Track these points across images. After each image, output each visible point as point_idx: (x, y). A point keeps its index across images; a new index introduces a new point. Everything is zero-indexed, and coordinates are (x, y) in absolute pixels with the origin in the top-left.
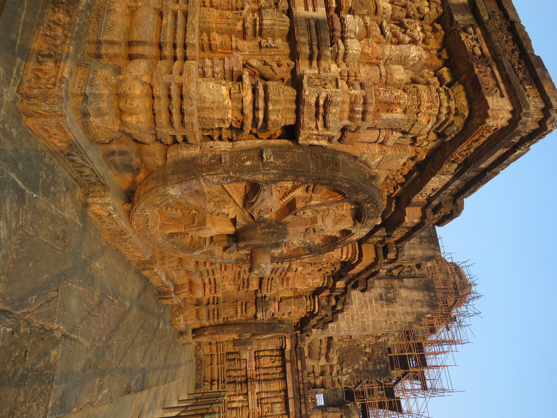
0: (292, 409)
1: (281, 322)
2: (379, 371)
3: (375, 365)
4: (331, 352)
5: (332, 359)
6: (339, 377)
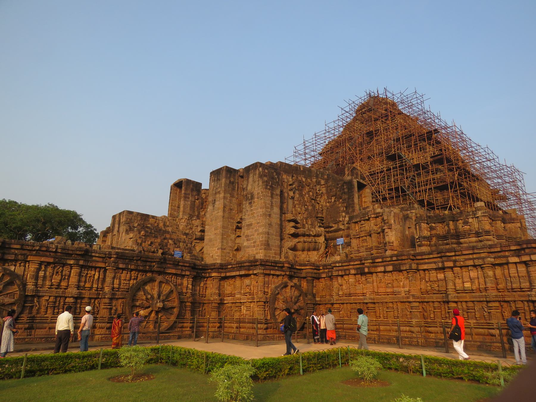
3: (345, 193)
4: (311, 233)
6: (345, 223)
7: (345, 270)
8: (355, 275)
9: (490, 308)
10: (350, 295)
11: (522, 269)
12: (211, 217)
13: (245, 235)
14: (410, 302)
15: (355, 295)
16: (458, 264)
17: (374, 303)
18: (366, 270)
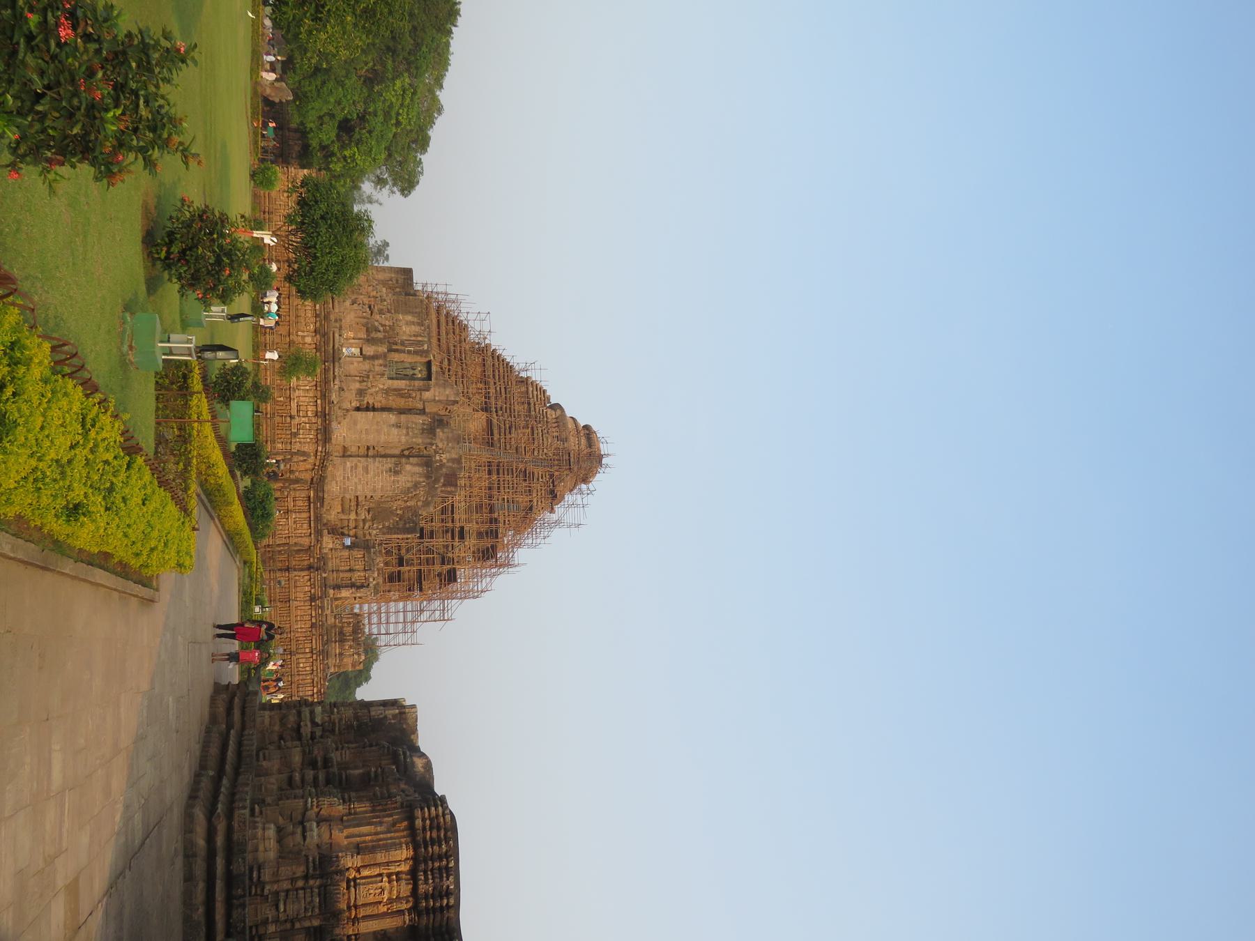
0: (312, 526)
1: (302, 480)
2: (408, 529)
5: (360, 514)
7: (314, 584)
8: (310, 591)
11: (310, 693)
12: (382, 422)
13: (359, 464)
14: (290, 632)
16: (314, 661)
17: (289, 607)
18: (313, 604)
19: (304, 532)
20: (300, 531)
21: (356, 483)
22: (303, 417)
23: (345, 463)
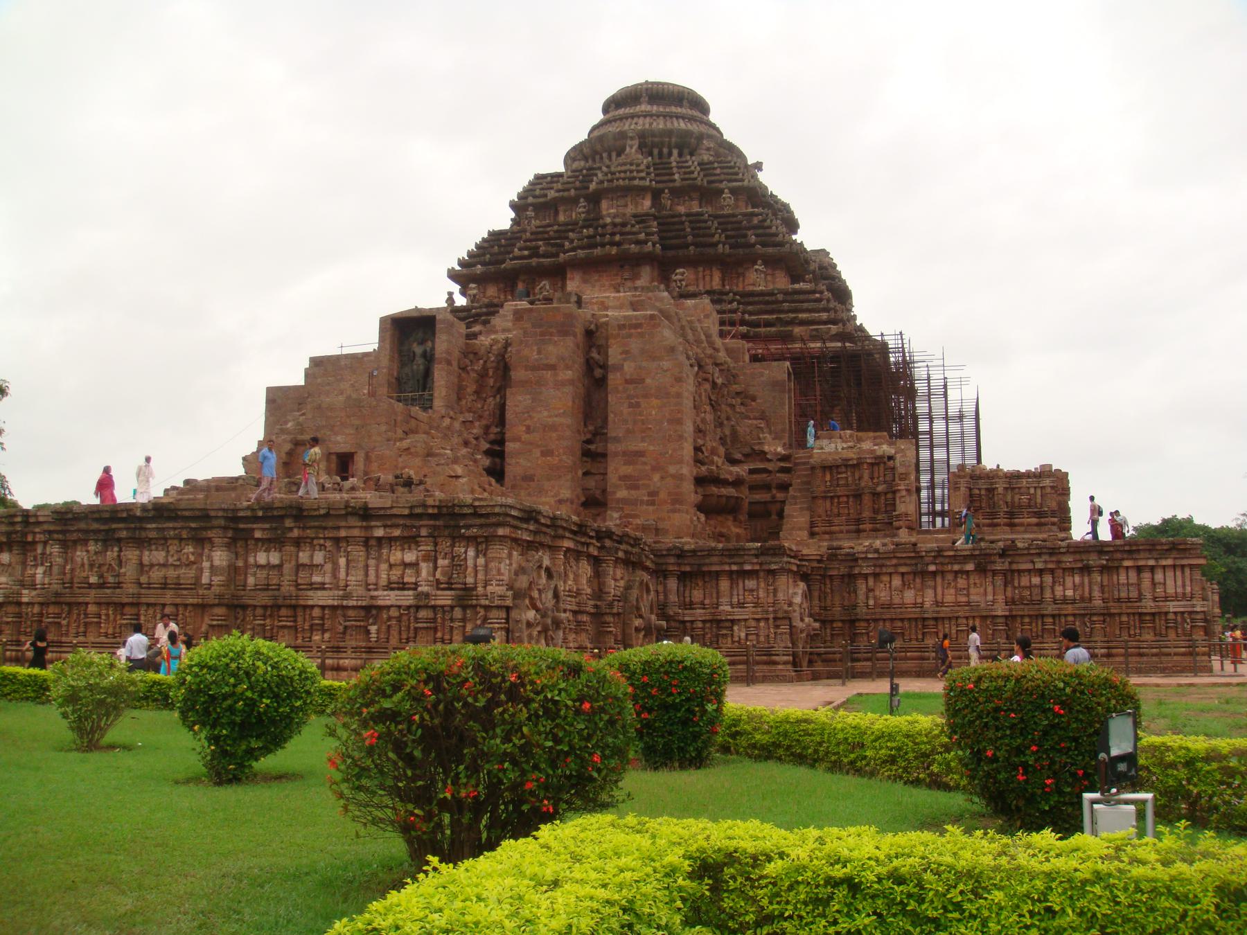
9: (1093, 622)
10: (890, 606)
11: (1133, 575)
15: (902, 605)
19: (762, 585)
20: (762, 594)
21: (662, 478)
22: (418, 573)
23: (618, 501)
